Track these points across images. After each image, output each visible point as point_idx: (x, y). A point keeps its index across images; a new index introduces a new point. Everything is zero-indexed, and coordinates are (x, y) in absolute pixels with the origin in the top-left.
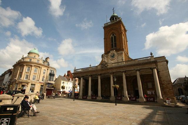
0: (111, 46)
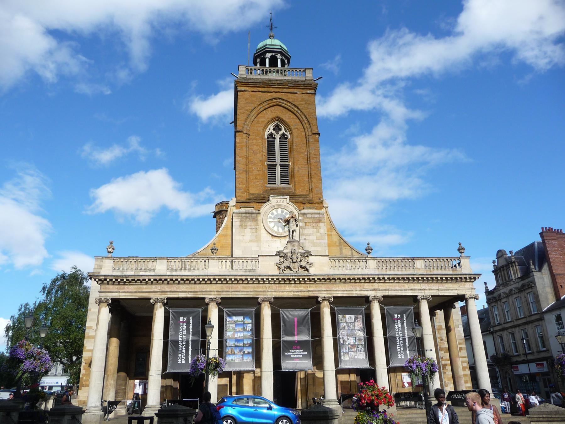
0: (266, 171)
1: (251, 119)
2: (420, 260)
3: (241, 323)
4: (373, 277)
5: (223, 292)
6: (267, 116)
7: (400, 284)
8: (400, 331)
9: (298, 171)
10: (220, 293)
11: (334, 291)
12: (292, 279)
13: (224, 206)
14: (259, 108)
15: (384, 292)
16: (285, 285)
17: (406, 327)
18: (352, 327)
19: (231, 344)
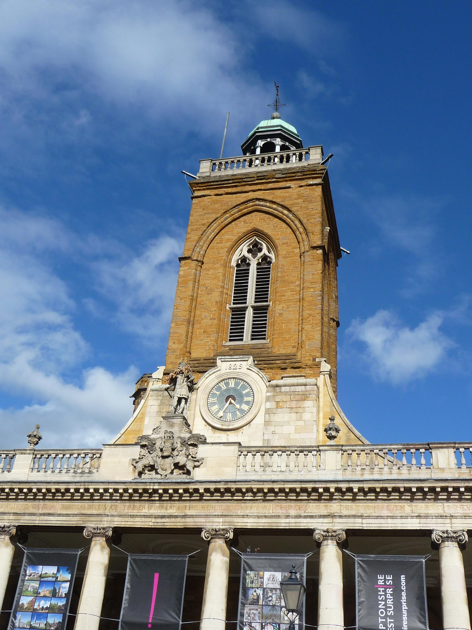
0: (228, 320)
1: (208, 237)
2: (446, 450)
3: (50, 579)
4: (324, 486)
5: (24, 514)
6: (235, 231)
7: (392, 505)
8: (391, 617)
9: (281, 314)
10: (19, 517)
11: (238, 516)
12: (153, 489)
13: (146, 381)
14: (222, 219)
15: (352, 520)
16: (143, 504)
17: (405, 607)
18: (274, 599)
19: (24, 624)
